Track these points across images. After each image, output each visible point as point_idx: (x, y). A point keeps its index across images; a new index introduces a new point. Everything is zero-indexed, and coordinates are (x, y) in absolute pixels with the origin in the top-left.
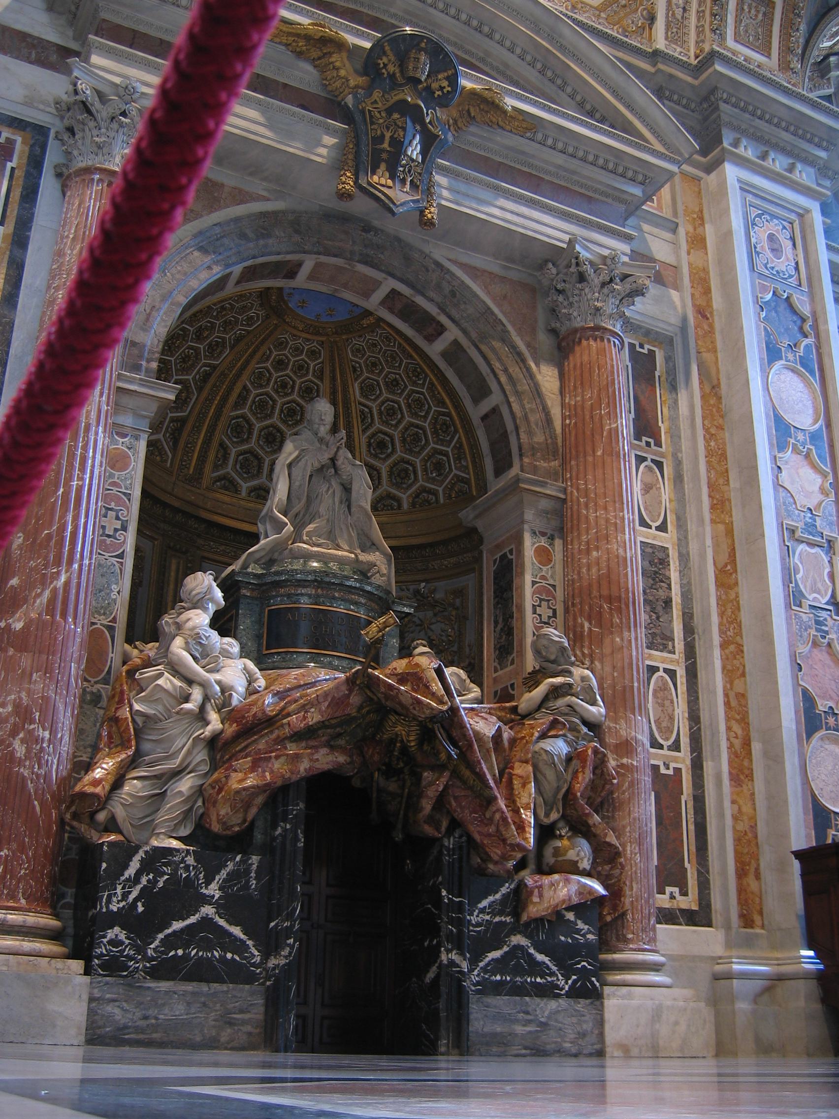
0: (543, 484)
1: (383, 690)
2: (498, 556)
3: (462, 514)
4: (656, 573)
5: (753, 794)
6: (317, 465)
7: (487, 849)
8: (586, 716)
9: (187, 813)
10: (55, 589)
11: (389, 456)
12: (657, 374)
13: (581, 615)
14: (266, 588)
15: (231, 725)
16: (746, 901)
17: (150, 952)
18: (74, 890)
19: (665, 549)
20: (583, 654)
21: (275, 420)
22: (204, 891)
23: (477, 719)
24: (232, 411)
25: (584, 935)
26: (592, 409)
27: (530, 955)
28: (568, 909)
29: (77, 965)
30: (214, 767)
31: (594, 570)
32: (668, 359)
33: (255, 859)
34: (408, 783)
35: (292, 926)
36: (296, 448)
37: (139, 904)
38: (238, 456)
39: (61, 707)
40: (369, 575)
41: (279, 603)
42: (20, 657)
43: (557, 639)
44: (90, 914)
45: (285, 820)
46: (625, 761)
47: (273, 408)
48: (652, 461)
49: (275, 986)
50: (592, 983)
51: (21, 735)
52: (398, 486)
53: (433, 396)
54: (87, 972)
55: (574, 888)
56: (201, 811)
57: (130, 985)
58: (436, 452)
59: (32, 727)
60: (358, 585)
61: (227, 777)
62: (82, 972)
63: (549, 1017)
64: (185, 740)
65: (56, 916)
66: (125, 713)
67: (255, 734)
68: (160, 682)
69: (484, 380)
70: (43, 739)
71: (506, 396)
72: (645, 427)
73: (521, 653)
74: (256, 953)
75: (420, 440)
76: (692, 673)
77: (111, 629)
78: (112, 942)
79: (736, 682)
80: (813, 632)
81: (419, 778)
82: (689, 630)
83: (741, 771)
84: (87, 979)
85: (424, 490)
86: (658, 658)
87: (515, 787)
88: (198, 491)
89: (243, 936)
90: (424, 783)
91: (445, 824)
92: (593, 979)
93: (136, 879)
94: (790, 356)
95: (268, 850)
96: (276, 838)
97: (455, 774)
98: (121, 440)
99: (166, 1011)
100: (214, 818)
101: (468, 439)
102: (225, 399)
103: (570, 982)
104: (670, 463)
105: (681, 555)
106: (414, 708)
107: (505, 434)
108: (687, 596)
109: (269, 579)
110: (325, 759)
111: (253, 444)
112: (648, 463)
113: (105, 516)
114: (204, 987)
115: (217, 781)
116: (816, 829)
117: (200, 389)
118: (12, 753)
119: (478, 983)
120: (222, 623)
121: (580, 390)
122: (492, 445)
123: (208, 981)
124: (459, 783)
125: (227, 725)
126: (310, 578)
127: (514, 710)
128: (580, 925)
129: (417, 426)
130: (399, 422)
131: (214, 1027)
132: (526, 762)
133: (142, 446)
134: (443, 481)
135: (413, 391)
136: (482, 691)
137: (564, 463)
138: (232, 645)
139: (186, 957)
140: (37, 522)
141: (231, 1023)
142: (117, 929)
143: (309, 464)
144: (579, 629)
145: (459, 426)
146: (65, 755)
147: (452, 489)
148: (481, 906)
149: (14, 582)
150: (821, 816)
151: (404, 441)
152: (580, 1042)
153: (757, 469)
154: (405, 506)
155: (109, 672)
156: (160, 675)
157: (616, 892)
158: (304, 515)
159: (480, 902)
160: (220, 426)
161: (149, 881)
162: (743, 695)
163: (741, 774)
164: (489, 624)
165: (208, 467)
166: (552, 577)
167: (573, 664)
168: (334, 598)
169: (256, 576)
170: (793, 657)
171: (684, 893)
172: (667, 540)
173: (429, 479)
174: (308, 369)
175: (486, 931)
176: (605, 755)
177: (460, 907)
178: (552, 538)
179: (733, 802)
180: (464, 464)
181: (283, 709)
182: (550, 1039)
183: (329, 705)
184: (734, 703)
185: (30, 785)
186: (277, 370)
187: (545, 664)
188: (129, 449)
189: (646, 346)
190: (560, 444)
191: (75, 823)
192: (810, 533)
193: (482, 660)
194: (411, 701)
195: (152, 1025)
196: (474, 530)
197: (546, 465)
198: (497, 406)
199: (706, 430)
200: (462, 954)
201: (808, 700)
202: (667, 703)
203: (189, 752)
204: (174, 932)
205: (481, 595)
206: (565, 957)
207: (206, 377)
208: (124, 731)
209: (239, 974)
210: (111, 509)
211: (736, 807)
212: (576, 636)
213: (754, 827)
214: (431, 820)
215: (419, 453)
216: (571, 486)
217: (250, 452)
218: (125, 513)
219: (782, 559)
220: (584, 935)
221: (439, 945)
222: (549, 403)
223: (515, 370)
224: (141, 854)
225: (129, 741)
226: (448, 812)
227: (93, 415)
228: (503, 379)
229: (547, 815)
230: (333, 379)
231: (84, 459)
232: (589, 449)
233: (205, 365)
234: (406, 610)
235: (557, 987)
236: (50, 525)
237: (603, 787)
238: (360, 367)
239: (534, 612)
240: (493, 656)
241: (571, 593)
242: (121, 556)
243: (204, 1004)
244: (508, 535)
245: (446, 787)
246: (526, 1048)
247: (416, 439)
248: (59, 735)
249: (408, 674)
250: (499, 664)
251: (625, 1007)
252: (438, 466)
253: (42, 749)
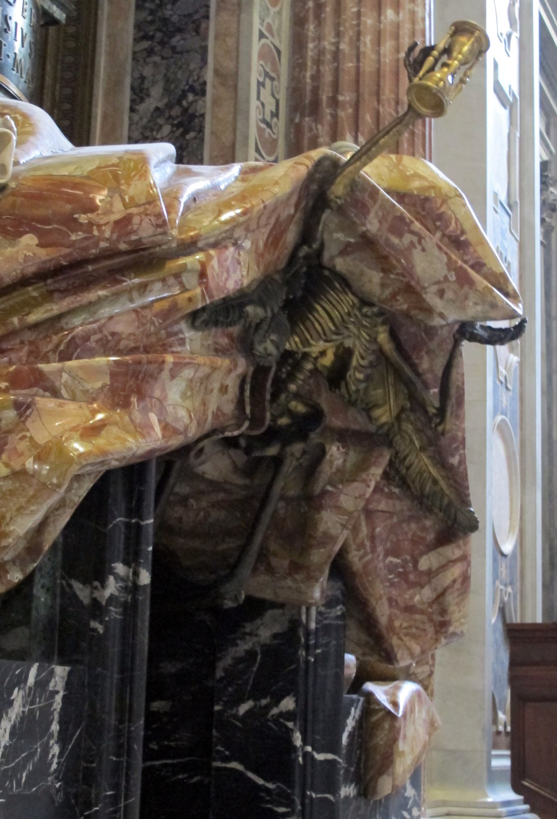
7: (395, 641)
31: (388, 46)
61: (23, 409)
67: (87, 284)
96: (97, 609)
106: (441, 294)
241: (328, 78)
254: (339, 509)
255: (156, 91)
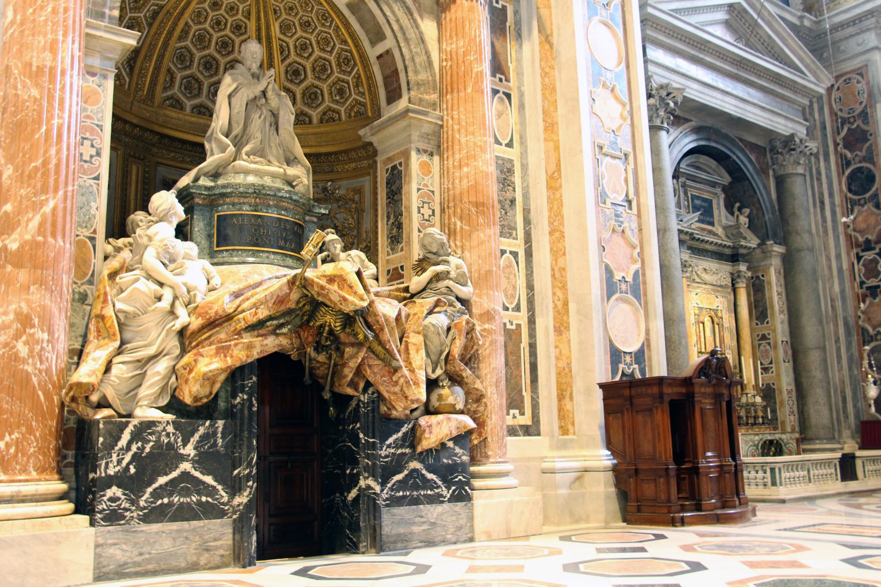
0: (425, 114)
1: (316, 289)
2: (390, 166)
3: (361, 132)
4: (505, 179)
5: (569, 340)
6: (252, 96)
8: (461, 295)
9: (163, 389)
10: (45, 213)
11: (302, 82)
12: (508, 24)
13: (454, 215)
14: (214, 199)
15: (197, 318)
16: (564, 416)
17: (142, 503)
18: (74, 452)
19: (511, 161)
20: (456, 245)
21: (212, 50)
22: (182, 451)
23: (384, 304)
24: (176, 43)
25: (460, 457)
26: (464, 55)
27: (423, 475)
28: (449, 440)
29: (84, 519)
30: (184, 351)
31: (465, 182)
32: (516, 13)
33: (220, 423)
34: (334, 356)
35: (251, 471)
36: (234, 80)
37: (131, 467)
38: (182, 80)
39: (56, 313)
40: (294, 184)
41: (225, 210)
42: (18, 273)
43: (439, 237)
44: (91, 476)
45: (243, 392)
46: (486, 326)
47: (210, 41)
48: (504, 93)
49: (240, 518)
50: (466, 491)
51: (24, 338)
52: (308, 105)
53: (338, 36)
54: (92, 523)
55: (453, 424)
56: (175, 386)
57: (127, 531)
58: (339, 79)
59: (32, 331)
60: (288, 195)
61: (196, 361)
62: (88, 524)
63: (436, 519)
64: (160, 330)
65: (62, 479)
66: (109, 312)
67: (217, 326)
68: (136, 285)
69: (380, 27)
70: (42, 340)
71: (398, 41)
72: (498, 68)
73: (409, 243)
74: (224, 494)
75: (326, 70)
76: (529, 254)
77: (92, 239)
78: (112, 500)
79: (560, 260)
80: (613, 222)
81: (340, 351)
82: (527, 222)
83: (562, 324)
84: (93, 530)
85: (330, 109)
86: (506, 244)
87: (411, 352)
88: (151, 109)
89: (214, 484)
90: (346, 356)
91: (362, 385)
92: (467, 488)
93: (128, 448)
94: (603, 12)
95: (230, 414)
96: (235, 406)
97: (370, 349)
98: (91, 79)
99: (157, 547)
100: (187, 393)
101: (365, 72)
102: (170, 33)
103: (451, 491)
104: (517, 95)
105: (522, 165)
107: (396, 72)
108: (526, 196)
109: (217, 192)
110: (270, 344)
111: (194, 70)
112: (501, 95)
113: (82, 145)
114: (185, 525)
115: (188, 364)
116: (612, 364)
117: (150, 25)
118: (16, 354)
119: (387, 499)
120: (182, 232)
121: (455, 39)
122: (386, 78)
123: (188, 520)
124: (372, 355)
125: (193, 318)
126: (250, 191)
127: (406, 290)
128: (458, 450)
129: (325, 59)
130: (310, 55)
131: (195, 554)
132: (419, 333)
133: (110, 84)
134: (344, 103)
135: (322, 31)
136: (377, 268)
137: (441, 96)
138: (190, 248)
139: (171, 504)
140: (24, 156)
141: (207, 550)
142: (114, 488)
143: (245, 95)
144: (452, 226)
145: (358, 61)
146: (61, 351)
147: (351, 110)
148: (388, 442)
149: (8, 207)
150: (616, 355)
151: (314, 69)
152: (458, 533)
153: (578, 102)
154: (315, 121)
155: (93, 275)
156: (137, 280)
157: (481, 424)
158: (242, 137)
159: (387, 439)
160: (168, 55)
161: (138, 448)
162: (564, 269)
163: (561, 328)
164: (382, 219)
165: (159, 88)
166: (432, 185)
167: (449, 255)
168: (269, 206)
169: (208, 188)
170: (600, 241)
171: (522, 414)
172: (512, 154)
173: (334, 101)
174: (238, 10)
175: (392, 461)
176: (474, 325)
177: (373, 446)
178: (431, 154)
179: (556, 347)
180: (361, 89)
181: (239, 306)
182: (437, 534)
183: (274, 303)
184: (557, 275)
185: (35, 380)
186: (213, 10)
187: (429, 255)
188: (99, 86)
189: (500, 2)
190: (438, 80)
191: (74, 405)
192: (613, 149)
193: (377, 245)
194: (338, 299)
195: (147, 559)
196: (371, 144)
197: (426, 97)
198: (391, 49)
199: (543, 69)
200: (376, 480)
201: (609, 271)
202: (512, 276)
203: (163, 340)
204: (161, 486)
205: (375, 193)
206: (447, 473)
207: (155, 14)
208: (110, 327)
209: (213, 511)
210: (86, 139)
211: (558, 350)
212: (451, 233)
213: (569, 364)
214: (353, 384)
215: (326, 80)
216: (447, 115)
217: (192, 76)
218: (99, 141)
219: (595, 169)
220: (460, 457)
221: (358, 474)
222: (430, 47)
223: (405, 21)
224: (130, 428)
225: (114, 335)
226: (364, 376)
227: (68, 61)
228: (396, 27)
229: (434, 371)
230: (258, 19)
231: (62, 101)
232: (461, 87)
233: (153, 5)
234: (323, 211)
235: (442, 496)
236: (36, 160)
237: (472, 347)
238: (280, 10)
239: (419, 212)
240: (386, 243)
241: (446, 199)
242: (97, 178)
243: (187, 538)
244: (398, 151)
245: (363, 359)
246: (421, 542)
247: (324, 69)
248: (56, 336)
249: (335, 276)
250: (392, 249)
251: (487, 503)
252: (341, 92)
253: (42, 349)
254: (350, 367)
255: (392, 216)
